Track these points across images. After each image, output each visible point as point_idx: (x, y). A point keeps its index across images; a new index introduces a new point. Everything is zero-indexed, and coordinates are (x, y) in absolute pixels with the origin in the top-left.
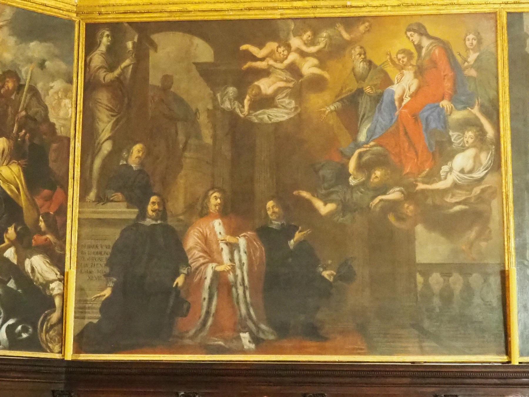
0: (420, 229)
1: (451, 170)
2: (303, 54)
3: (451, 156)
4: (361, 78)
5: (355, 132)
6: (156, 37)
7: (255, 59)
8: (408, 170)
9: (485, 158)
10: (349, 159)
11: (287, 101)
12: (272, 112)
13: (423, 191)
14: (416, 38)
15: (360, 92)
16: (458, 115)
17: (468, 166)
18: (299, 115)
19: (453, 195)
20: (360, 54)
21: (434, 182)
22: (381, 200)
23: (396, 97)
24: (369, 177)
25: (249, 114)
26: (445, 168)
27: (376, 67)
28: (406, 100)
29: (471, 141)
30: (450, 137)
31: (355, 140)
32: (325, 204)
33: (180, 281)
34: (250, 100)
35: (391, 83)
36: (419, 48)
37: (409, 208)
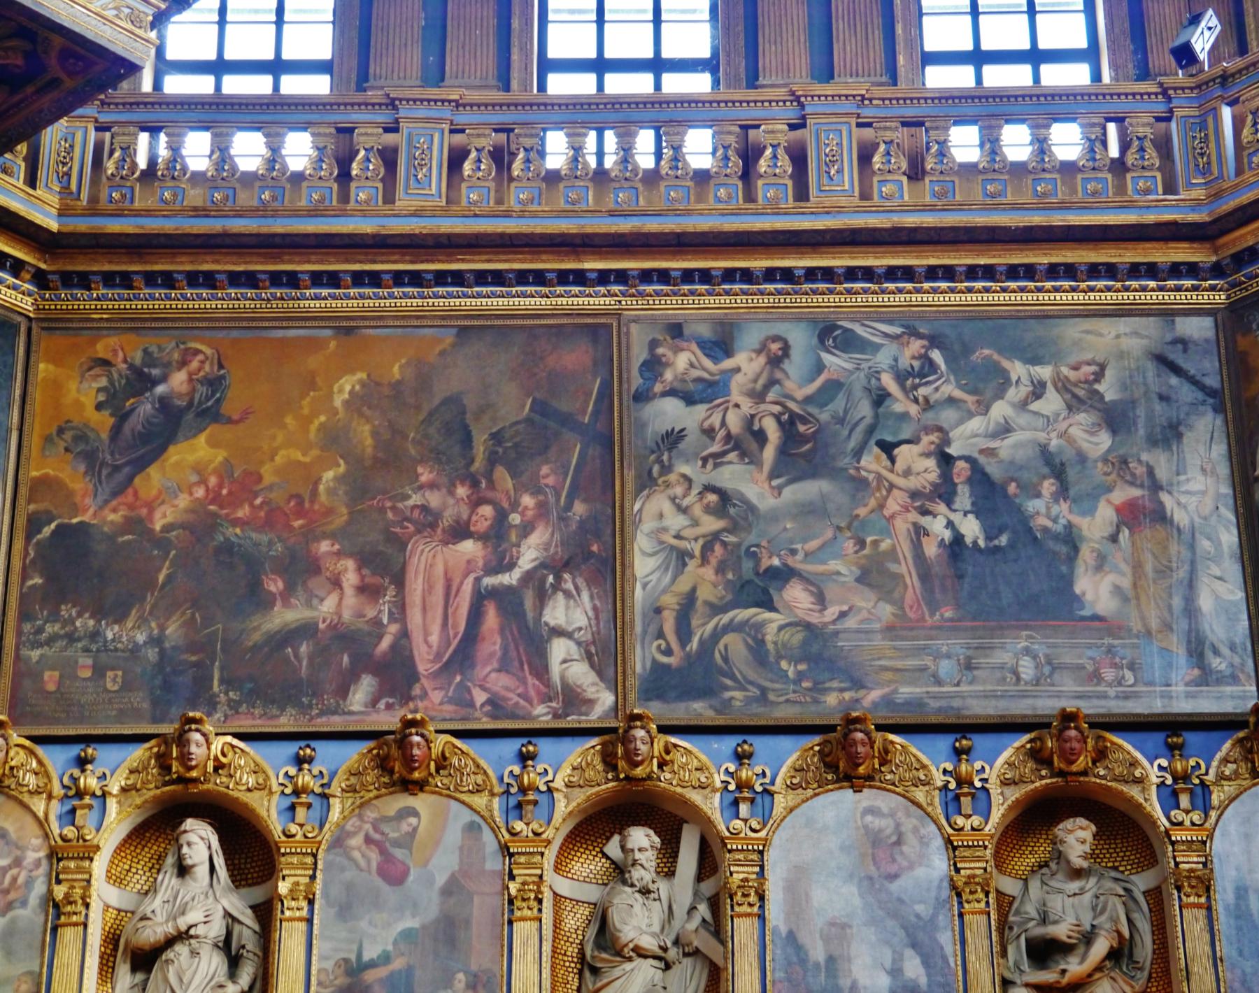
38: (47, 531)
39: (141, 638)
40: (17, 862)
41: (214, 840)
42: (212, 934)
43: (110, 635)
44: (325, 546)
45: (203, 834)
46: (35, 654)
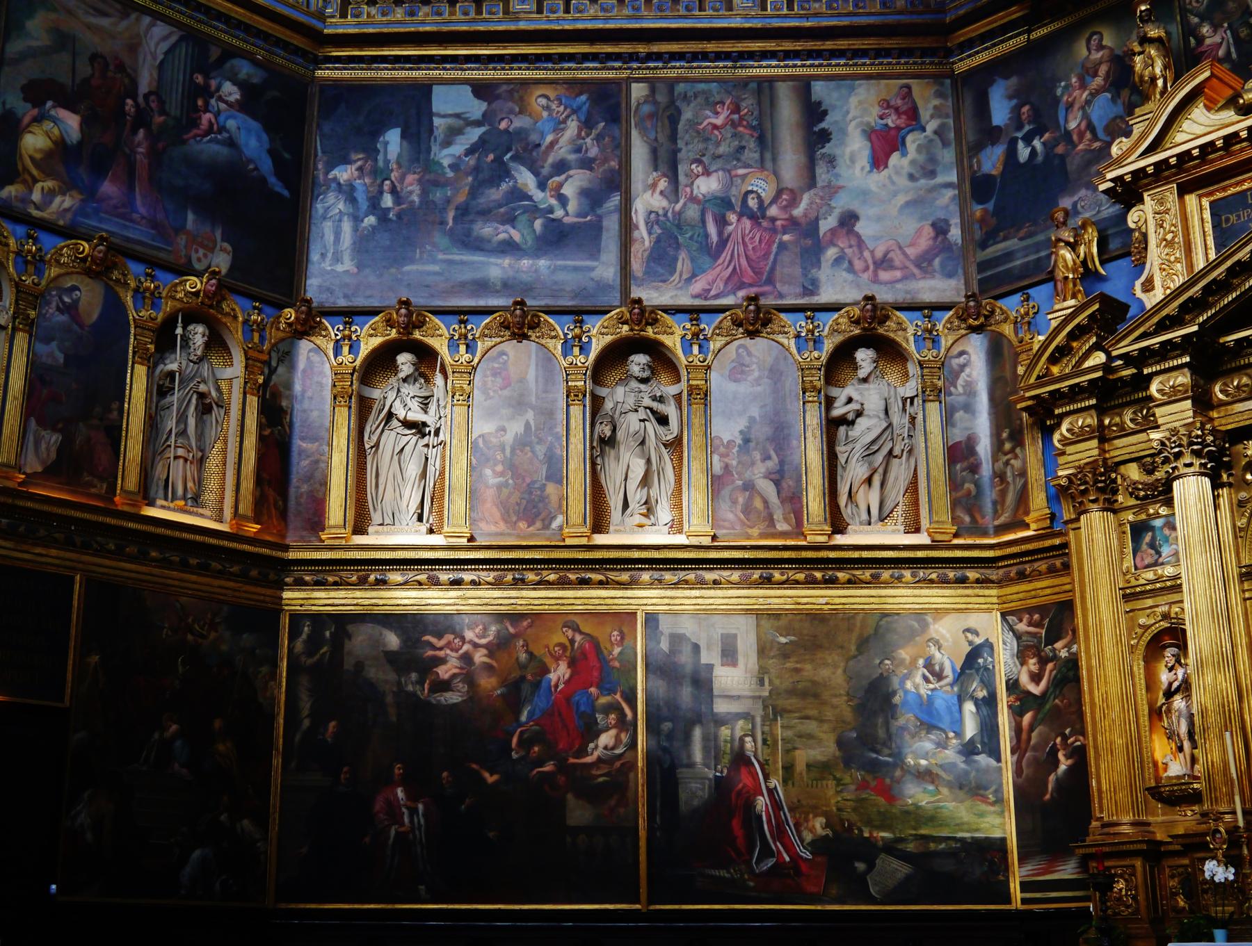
0: (570, 796)
1: (597, 747)
2: (476, 646)
3: (597, 736)
4: (523, 667)
5: (518, 713)
6: (350, 628)
7: (434, 648)
8: (561, 746)
9: (625, 737)
10: (512, 736)
11: (461, 685)
12: (448, 695)
13: (573, 764)
14: (570, 633)
15: (523, 678)
16: (603, 700)
17: (611, 743)
18: (471, 699)
19: (598, 768)
20: (523, 646)
21: (584, 757)
22: (539, 772)
23: (553, 683)
24: (528, 753)
25: (429, 696)
26: (592, 745)
27: (535, 656)
28: (561, 686)
29: (613, 722)
30: (596, 719)
31: (517, 719)
32: (491, 775)
33: (367, 840)
34: (430, 684)
35: (548, 671)
36: (572, 641)
37: (561, 779)
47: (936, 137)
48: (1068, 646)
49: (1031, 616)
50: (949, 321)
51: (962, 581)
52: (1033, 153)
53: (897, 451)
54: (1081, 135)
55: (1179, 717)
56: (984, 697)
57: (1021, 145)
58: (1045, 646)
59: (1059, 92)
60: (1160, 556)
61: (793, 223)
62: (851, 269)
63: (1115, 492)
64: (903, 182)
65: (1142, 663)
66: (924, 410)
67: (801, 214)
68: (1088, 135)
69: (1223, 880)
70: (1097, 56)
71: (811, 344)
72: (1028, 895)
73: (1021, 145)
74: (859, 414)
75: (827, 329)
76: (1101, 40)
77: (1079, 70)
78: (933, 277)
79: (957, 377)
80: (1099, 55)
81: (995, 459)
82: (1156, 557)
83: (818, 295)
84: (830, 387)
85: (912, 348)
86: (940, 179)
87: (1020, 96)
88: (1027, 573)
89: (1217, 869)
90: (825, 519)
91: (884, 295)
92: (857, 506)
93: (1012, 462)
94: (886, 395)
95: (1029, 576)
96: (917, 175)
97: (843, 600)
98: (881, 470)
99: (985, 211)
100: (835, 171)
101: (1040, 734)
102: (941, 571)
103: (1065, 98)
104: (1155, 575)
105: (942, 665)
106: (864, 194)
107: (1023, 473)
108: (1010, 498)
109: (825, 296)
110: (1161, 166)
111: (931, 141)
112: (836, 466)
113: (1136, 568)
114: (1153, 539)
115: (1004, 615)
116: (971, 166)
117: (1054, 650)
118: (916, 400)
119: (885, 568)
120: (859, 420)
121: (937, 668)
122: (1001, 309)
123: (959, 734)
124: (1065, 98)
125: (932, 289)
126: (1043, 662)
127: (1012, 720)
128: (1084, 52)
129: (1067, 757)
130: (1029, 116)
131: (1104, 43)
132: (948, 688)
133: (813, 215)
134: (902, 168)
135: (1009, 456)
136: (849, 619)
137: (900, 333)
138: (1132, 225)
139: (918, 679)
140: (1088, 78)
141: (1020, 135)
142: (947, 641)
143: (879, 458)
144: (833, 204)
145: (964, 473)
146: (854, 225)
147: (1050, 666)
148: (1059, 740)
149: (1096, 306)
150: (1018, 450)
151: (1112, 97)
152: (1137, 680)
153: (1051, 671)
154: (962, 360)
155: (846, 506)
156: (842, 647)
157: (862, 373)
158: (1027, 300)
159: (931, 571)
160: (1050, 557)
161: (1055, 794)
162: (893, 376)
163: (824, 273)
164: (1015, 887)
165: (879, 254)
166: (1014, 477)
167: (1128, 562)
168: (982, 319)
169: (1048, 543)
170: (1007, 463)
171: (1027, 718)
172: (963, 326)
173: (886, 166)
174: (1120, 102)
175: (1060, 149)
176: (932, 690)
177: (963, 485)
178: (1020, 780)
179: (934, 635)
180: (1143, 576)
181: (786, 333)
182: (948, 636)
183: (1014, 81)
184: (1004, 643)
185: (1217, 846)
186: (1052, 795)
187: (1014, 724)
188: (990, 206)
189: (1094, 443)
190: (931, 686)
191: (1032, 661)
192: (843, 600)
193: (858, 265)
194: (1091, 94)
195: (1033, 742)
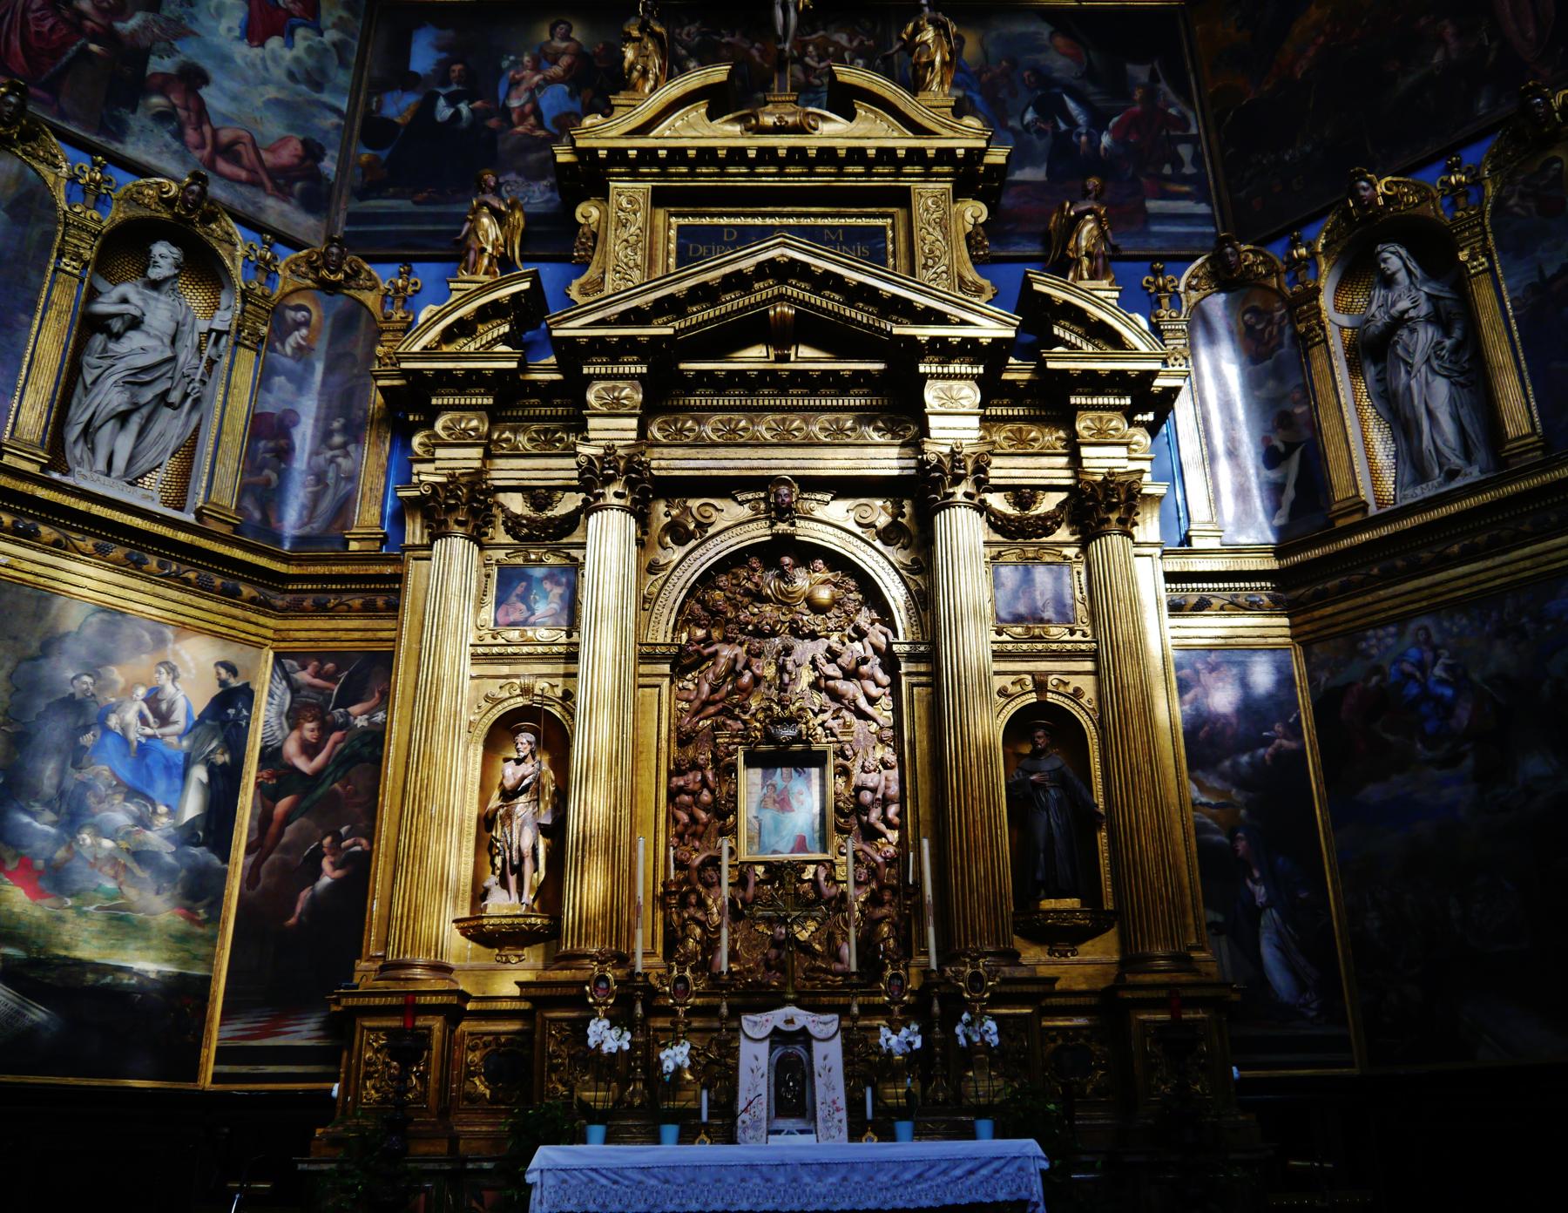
38: (1229, 119)
39: (1308, 148)
40: (1270, 322)
41: (1403, 252)
42: (1423, 313)
43: (1287, 158)
44: (1423, 21)
45: (1392, 249)
46: (1242, 194)
47: (333, 50)
48: (370, 712)
49: (322, 664)
50: (294, 261)
51: (230, 594)
52: (457, 115)
53: (175, 397)
54: (523, 117)
55: (522, 826)
56: (224, 764)
57: (442, 102)
58: (334, 708)
59: (505, 64)
60: (533, 614)
61: (109, 37)
62: (179, 135)
63: (489, 522)
64: (278, 73)
65: (480, 749)
66: (234, 355)
67: (126, 32)
68: (532, 120)
69: (614, 1050)
70: (561, 45)
71: (91, 198)
72: (226, 1069)
73: (442, 102)
74: (135, 323)
75: (122, 190)
76: (570, 29)
77: (536, 51)
78: (289, 203)
79: (290, 334)
80: (564, 45)
81: (315, 453)
82: (526, 614)
83: (122, 142)
84: (98, 276)
85: (237, 271)
86: (326, 97)
87: (452, 53)
88: (330, 605)
89: (606, 1033)
90: (42, 442)
91: (217, 190)
92: (93, 450)
93: (340, 460)
94: (180, 318)
95: (332, 609)
96: (298, 76)
97: (38, 569)
98: (145, 411)
99: (376, 159)
100: (194, 10)
101: (300, 829)
102: (203, 572)
103: (511, 73)
104: (522, 636)
105: (172, 704)
106: (225, 59)
107: (352, 478)
108: (326, 503)
109: (133, 150)
110: (648, 155)
111: (326, 50)
112: (75, 384)
113: (496, 623)
114: (528, 590)
115: (278, 657)
116: (368, 104)
117: (348, 714)
118: (224, 340)
119: (120, 543)
120: (131, 334)
121: (164, 706)
122: (369, 273)
123: (173, 812)
124: (511, 73)
125: (282, 214)
126: (326, 729)
127: (259, 805)
128: (546, 36)
129: (335, 866)
130: (460, 76)
131: (572, 35)
132: (174, 740)
133: (145, 43)
134: (282, 58)
135: (337, 452)
136: (40, 598)
137: (226, 245)
138: (582, 221)
139: (131, 716)
140: (544, 63)
141: (443, 91)
142: (189, 671)
143: (148, 394)
144: (177, 45)
145: (268, 456)
146: (200, 87)
147: (336, 736)
148: (327, 841)
149: (526, 286)
150: (351, 448)
151: (571, 92)
152: (470, 767)
153: (336, 743)
154: (300, 315)
155: (76, 442)
156: (15, 638)
157: (154, 274)
158: (409, 273)
159: (188, 567)
160: (370, 591)
161: (304, 918)
162: (195, 298)
163: (138, 120)
164: (209, 1054)
165: (226, 136)
166: (338, 479)
167: (488, 613)
168: (341, 276)
169: (374, 569)
170: (332, 460)
171: (284, 804)
172: (311, 276)
173: (262, 45)
174: (578, 99)
175: (493, 123)
176: (149, 737)
177: (261, 469)
178: (251, 894)
179: (170, 658)
180: (505, 635)
181: (57, 166)
182: (191, 665)
183: (449, 33)
184: (271, 695)
185: (601, 1000)
186: (299, 919)
187: (259, 811)
188: (384, 154)
189: (477, 452)
190: (148, 731)
191: (309, 726)
192: (38, 569)
193: (191, 135)
194: (544, 79)
195: (284, 840)
